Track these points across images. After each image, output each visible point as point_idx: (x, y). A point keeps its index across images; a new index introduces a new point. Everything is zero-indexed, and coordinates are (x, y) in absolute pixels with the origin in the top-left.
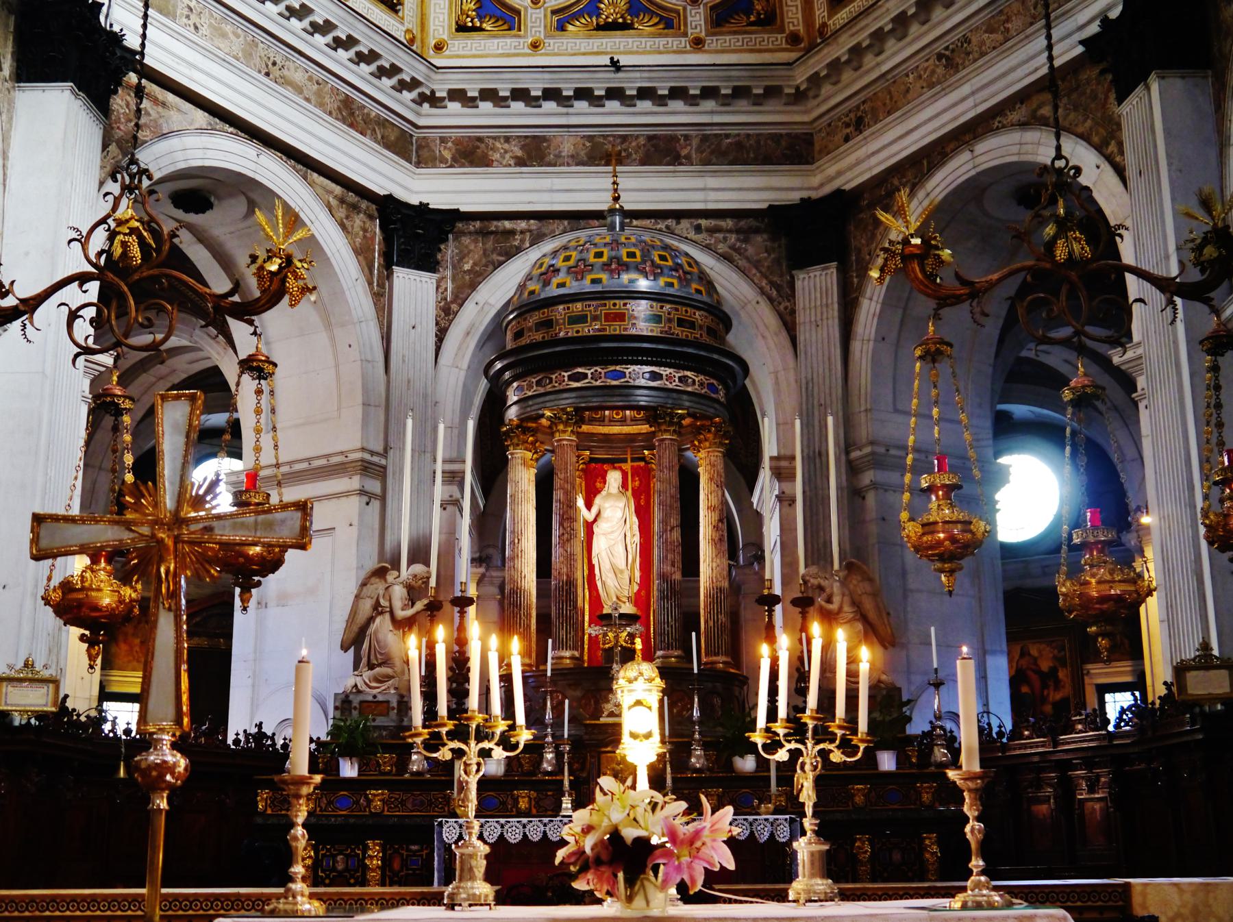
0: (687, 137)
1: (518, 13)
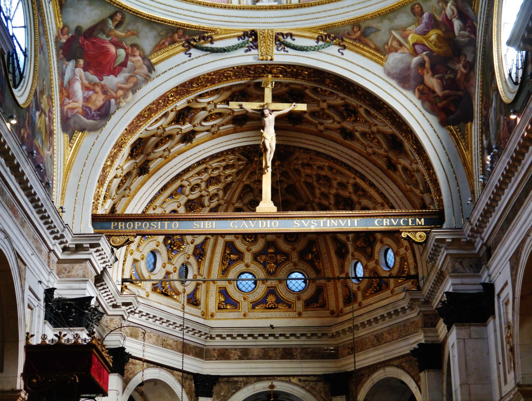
0: (296, 348)
1: (239, 303)
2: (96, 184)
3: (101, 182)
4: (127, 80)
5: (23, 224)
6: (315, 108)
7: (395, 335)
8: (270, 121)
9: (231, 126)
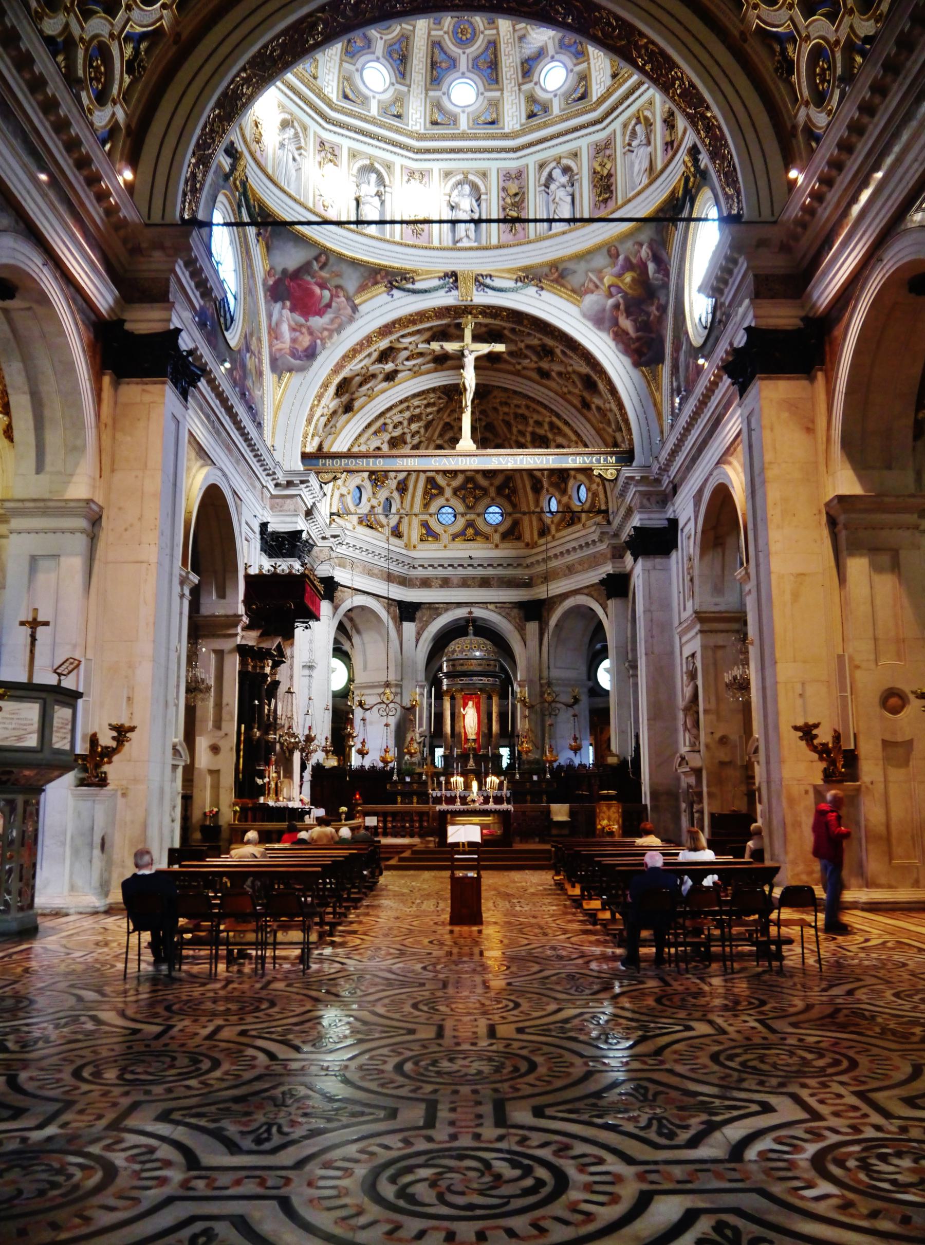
2: (304, 423)
3: (309, 421)
4: (332, 321)
5: (238, 462)
6: (514, 348)
7: (586, 566)
8: (469, 361)
9: (431, 365)
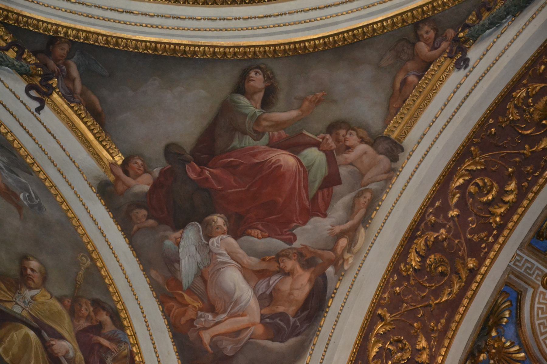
4: (351, 209)
